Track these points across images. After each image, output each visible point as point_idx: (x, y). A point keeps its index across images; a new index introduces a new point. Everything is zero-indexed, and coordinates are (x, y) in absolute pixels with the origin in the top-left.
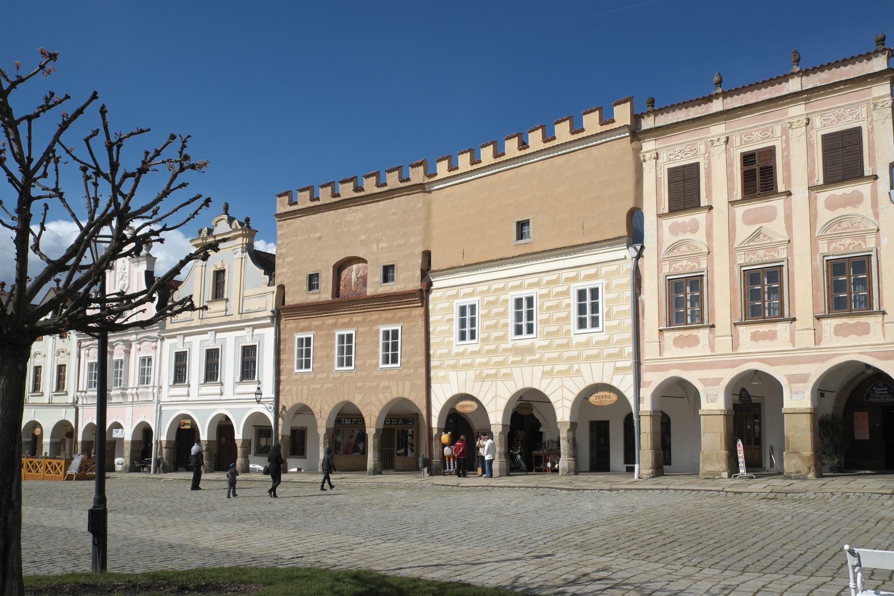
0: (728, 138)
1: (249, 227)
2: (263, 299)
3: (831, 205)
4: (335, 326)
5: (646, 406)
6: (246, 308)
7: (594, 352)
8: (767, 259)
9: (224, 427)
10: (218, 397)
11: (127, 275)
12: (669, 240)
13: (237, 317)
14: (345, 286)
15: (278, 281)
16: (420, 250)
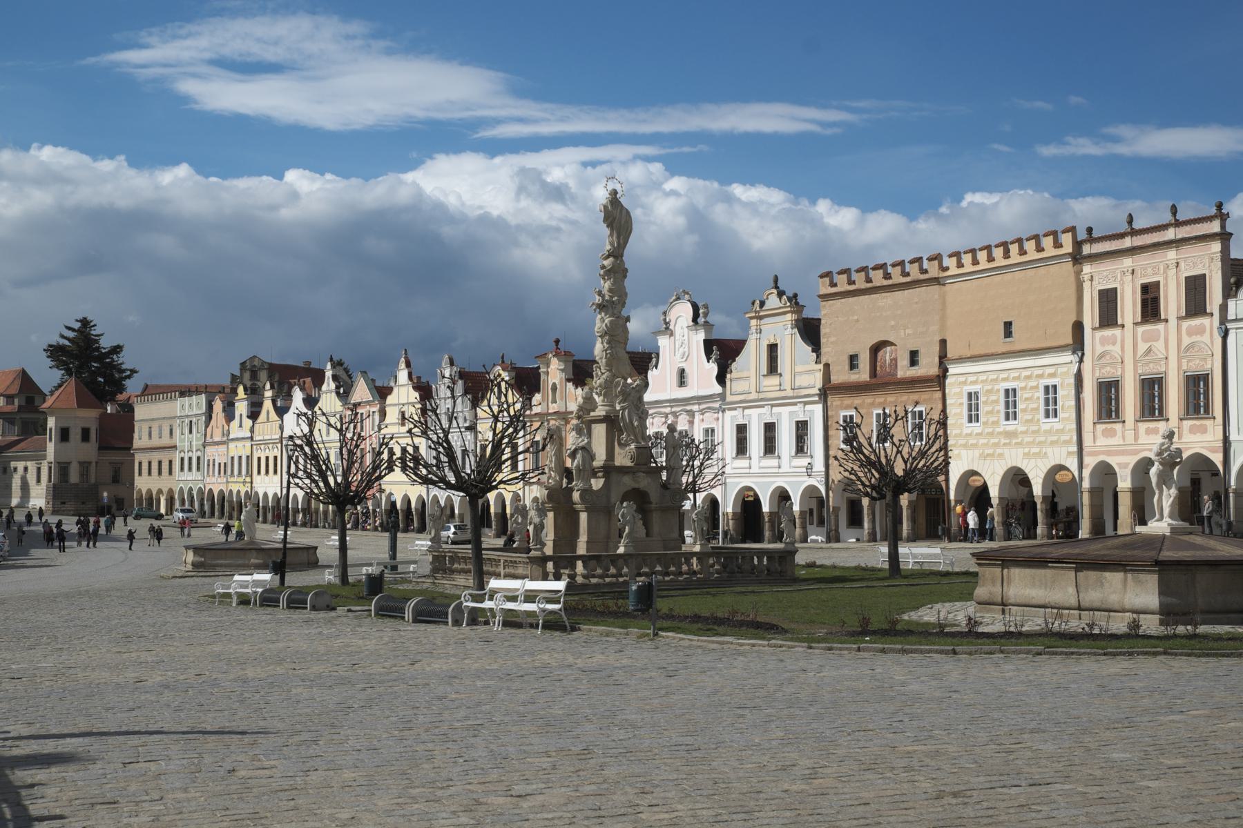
0: (1133, 270)
1: (797, 303)
2: (812, 376)
3: (1190, 333)
4: (873, 405)
5: (1086, 484)
6: (797, 384)
7: (1055, 438)
8: (1154, 371)
9: (783, 497)
10: (776, 470)
11: (686, 342)
12: (1099, 349)
13: (789, 393)
14: (881, 367)
15: (824, 360)
16: (938, 338)
